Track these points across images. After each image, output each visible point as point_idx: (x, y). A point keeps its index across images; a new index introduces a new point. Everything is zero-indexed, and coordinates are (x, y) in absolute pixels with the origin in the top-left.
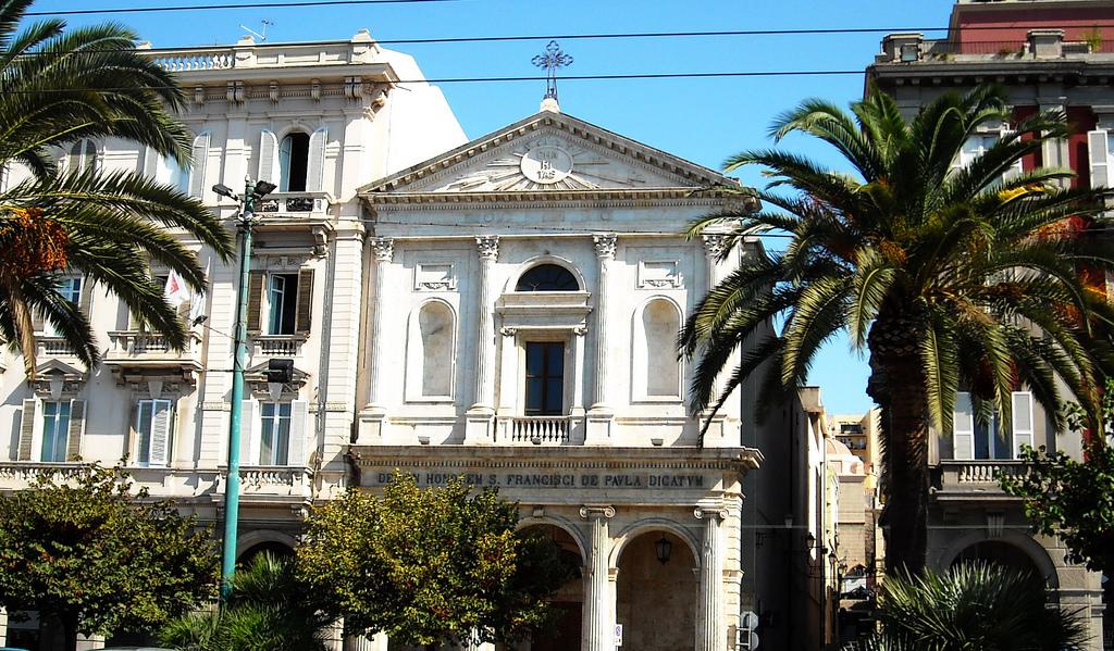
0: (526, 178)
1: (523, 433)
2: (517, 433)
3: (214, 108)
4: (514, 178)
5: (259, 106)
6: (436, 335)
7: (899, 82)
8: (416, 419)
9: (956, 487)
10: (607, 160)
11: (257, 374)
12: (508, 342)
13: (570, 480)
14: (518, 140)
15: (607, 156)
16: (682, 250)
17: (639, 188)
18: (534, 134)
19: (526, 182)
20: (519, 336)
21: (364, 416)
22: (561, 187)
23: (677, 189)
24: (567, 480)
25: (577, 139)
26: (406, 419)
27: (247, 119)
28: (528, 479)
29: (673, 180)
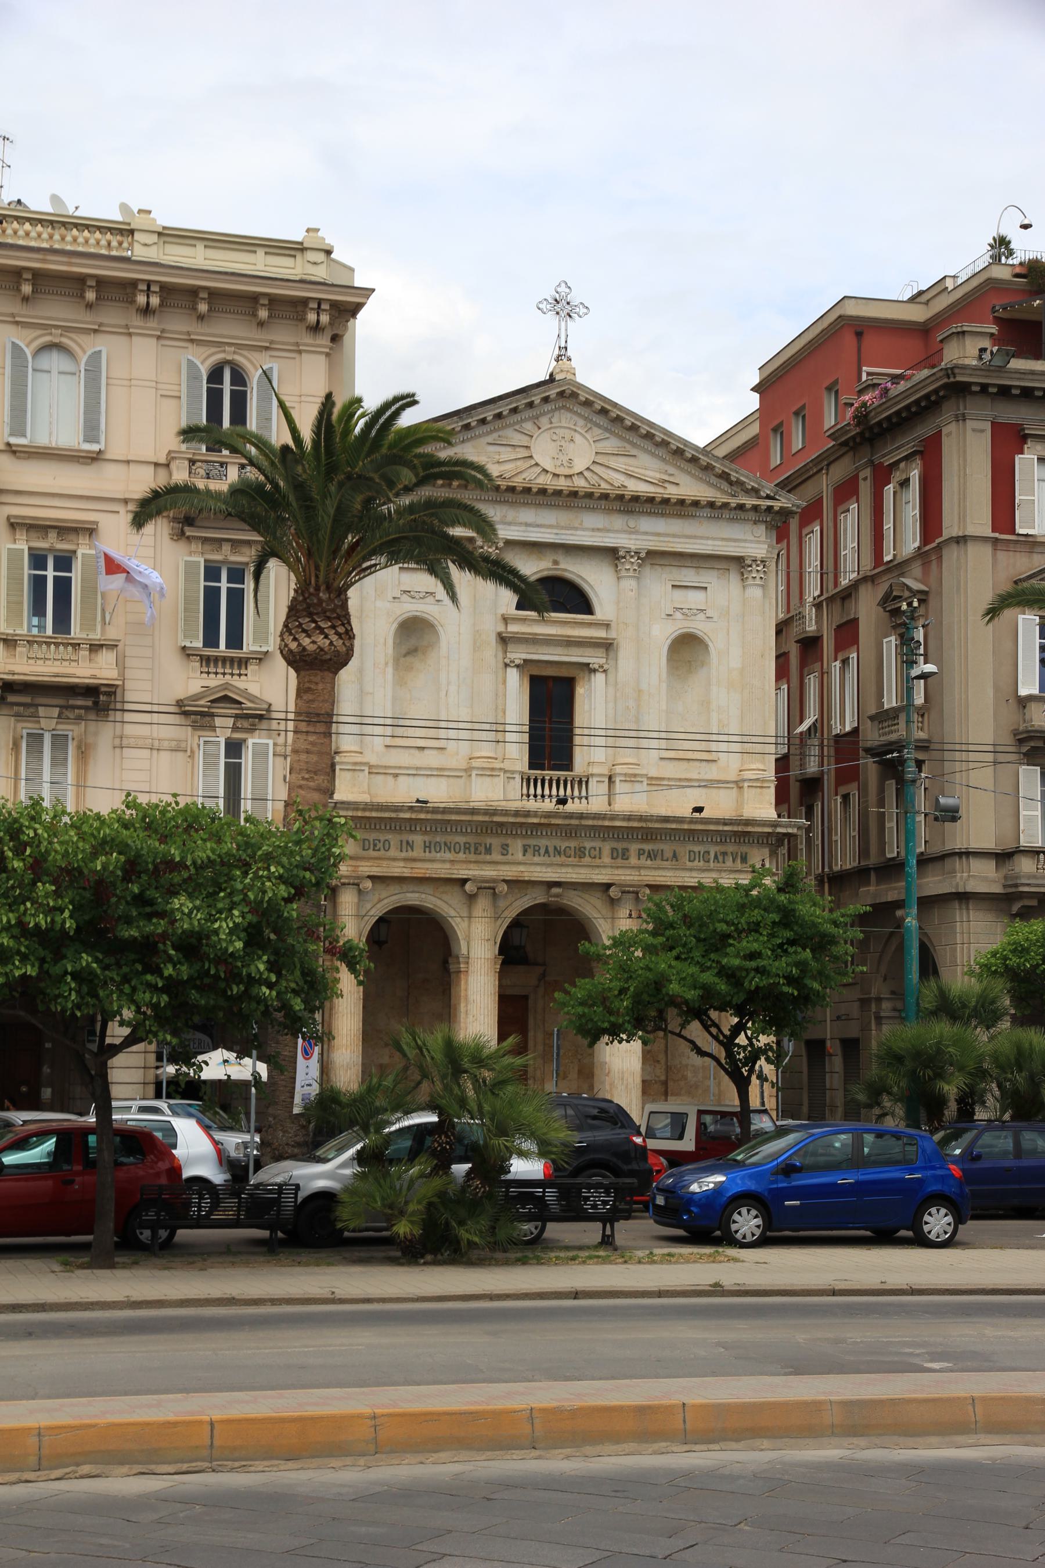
0: (537, 464)
1: (539, 791)
2: (525, 791)
3: (112, 316)
4: (519, 463)
5: (179, 323)
6: (409, 659)
7: (976, 389)
8: (400, 768)
9: (1035, 877)
10: (634, 452)
11: (202, 702)
12: (513, 674)
13: (597, 853)
14: (530, 413)
15: (634, 445)
16: (715, 573)
17: (673, 492)
18: (547, 407)
19: (538, 470)
20: (525, 665)
21: (342, 763)
22: (580, 483)
23: (721, 498)
24: (593, 853)
25: (601, 420)
26: (386, 767)
27: (159, 338)
28: (547, 851)
29: (712, 485)
